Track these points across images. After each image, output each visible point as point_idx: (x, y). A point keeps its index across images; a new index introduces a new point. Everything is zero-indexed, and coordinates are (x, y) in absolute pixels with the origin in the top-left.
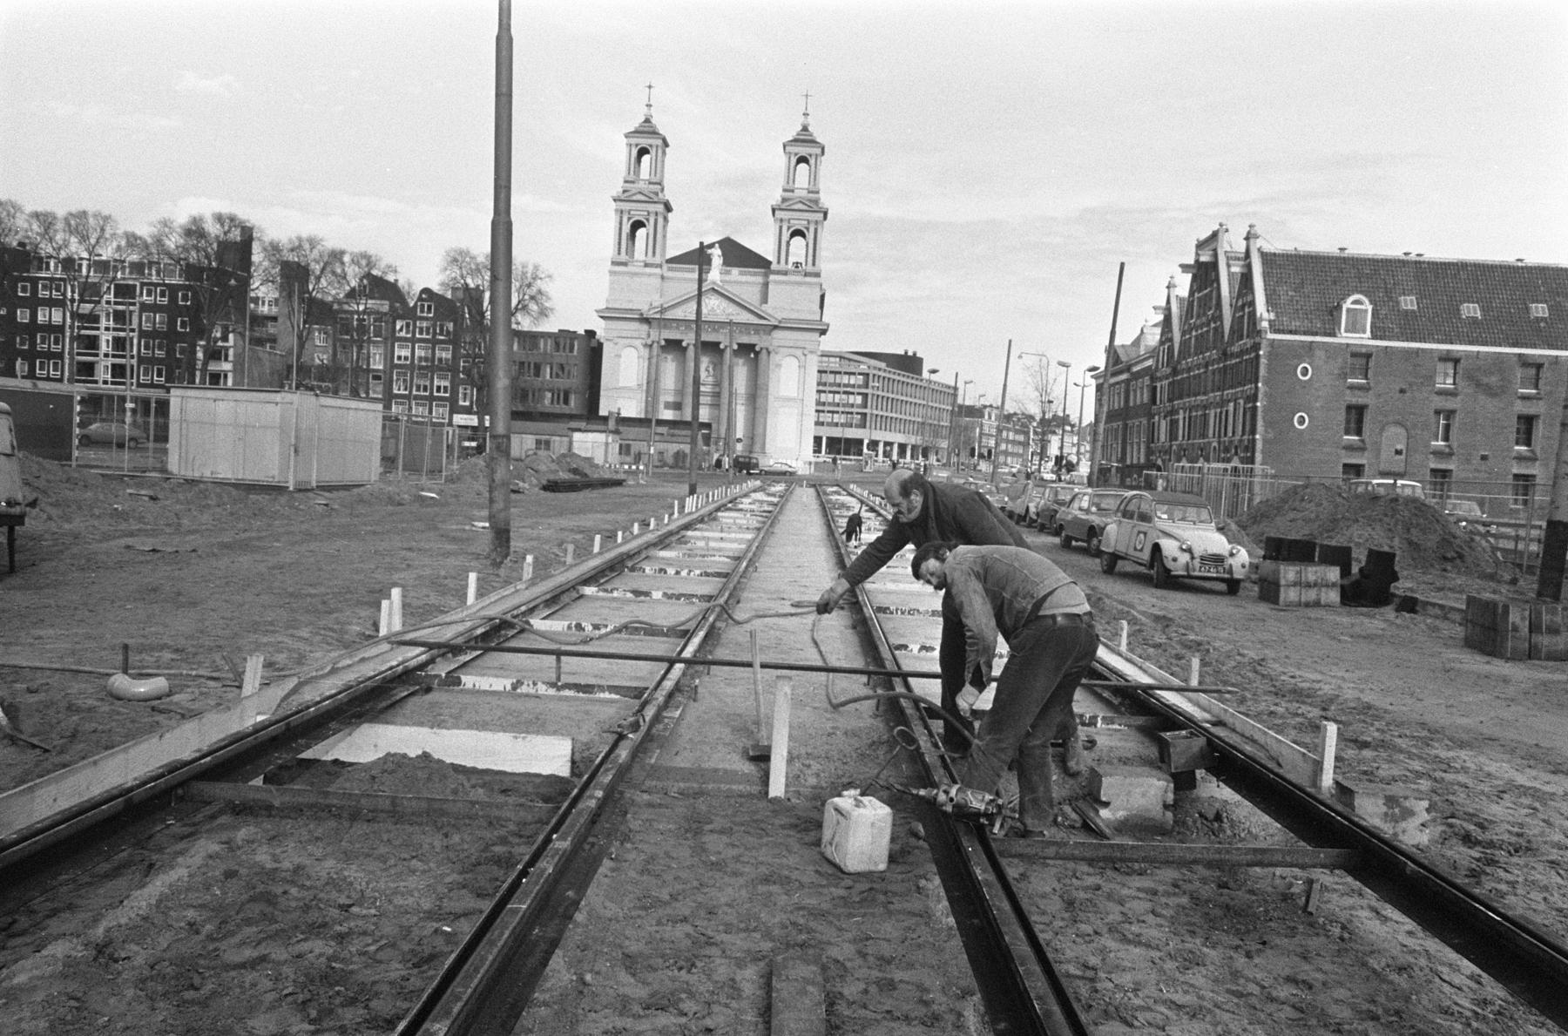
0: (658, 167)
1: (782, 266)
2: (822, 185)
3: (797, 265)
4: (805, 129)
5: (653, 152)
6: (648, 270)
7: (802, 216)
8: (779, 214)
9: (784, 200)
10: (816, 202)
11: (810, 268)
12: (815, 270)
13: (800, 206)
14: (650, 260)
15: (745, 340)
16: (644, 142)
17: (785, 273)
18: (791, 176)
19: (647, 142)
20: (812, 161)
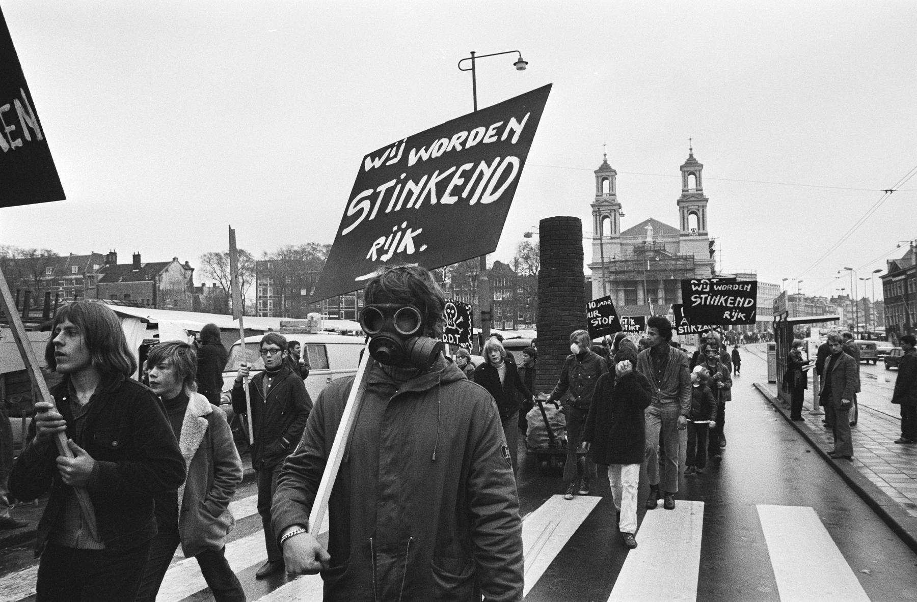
0: (612, 187)
1: (686, 232)
2: (704, 185)
3: (693, 230)
4: (691, 156)
6: (613, 241)
7: (692, 203)
8: (682, 204)
9: (684, 196)
10: (702, 195)
11: (701, 231)
12: (704, 232)
13: (693, 199)
16: (605, 174)
17: (688, 235)
20: (697, 174)
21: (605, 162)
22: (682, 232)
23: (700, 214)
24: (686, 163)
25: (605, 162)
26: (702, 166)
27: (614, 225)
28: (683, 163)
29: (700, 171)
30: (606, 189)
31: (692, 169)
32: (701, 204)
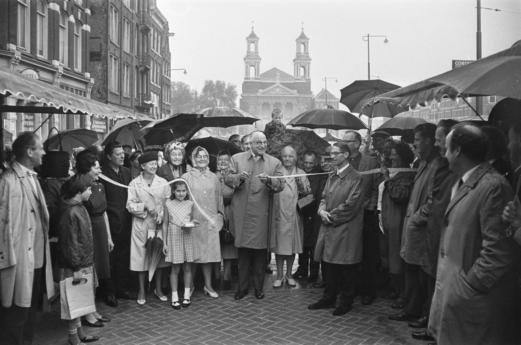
0: (256, 47)
1: (299, 78)
5: (256, 43)
10: (308, 57)
11: (307, 78)
14: (257, 77)
15: (289, 101)
17: (299, 80)
18: (298, 48)
19: (252, 38)
20: (306, 44)
21: (253, 32)
22: (296, 77)
23: (307, 68)
24: (300, 37)
25: (253, 32)
26: (309, 39)
27: (257, 71)
28: (298, 37)
29: (308, 42)
30: (252, 49)
31: (303, 41)
32: (307, 62)
